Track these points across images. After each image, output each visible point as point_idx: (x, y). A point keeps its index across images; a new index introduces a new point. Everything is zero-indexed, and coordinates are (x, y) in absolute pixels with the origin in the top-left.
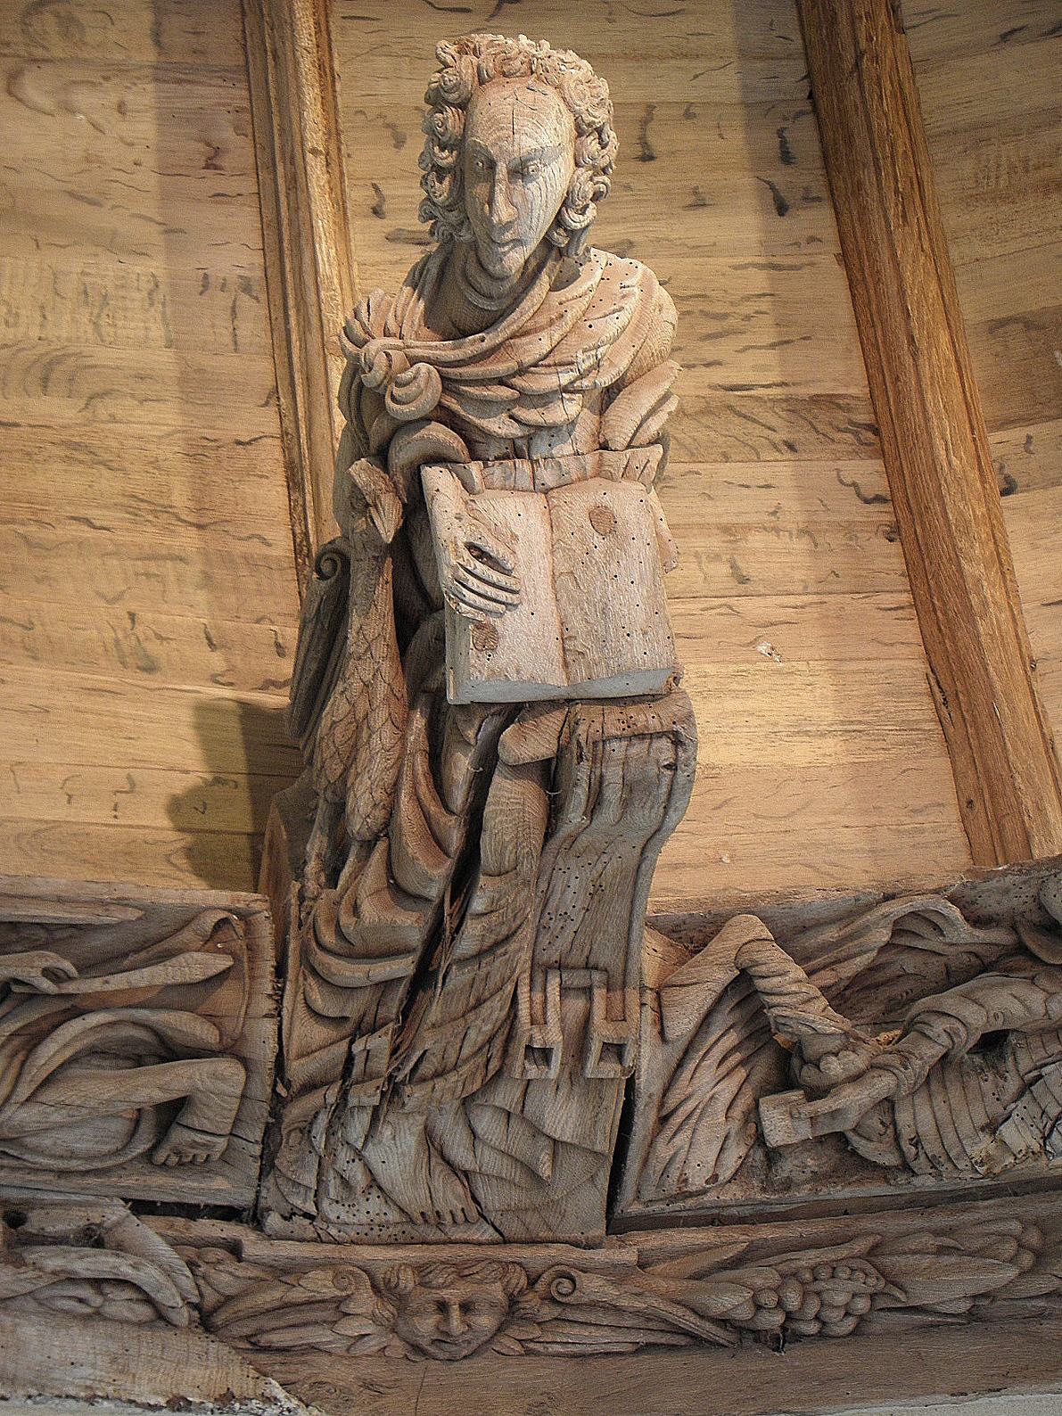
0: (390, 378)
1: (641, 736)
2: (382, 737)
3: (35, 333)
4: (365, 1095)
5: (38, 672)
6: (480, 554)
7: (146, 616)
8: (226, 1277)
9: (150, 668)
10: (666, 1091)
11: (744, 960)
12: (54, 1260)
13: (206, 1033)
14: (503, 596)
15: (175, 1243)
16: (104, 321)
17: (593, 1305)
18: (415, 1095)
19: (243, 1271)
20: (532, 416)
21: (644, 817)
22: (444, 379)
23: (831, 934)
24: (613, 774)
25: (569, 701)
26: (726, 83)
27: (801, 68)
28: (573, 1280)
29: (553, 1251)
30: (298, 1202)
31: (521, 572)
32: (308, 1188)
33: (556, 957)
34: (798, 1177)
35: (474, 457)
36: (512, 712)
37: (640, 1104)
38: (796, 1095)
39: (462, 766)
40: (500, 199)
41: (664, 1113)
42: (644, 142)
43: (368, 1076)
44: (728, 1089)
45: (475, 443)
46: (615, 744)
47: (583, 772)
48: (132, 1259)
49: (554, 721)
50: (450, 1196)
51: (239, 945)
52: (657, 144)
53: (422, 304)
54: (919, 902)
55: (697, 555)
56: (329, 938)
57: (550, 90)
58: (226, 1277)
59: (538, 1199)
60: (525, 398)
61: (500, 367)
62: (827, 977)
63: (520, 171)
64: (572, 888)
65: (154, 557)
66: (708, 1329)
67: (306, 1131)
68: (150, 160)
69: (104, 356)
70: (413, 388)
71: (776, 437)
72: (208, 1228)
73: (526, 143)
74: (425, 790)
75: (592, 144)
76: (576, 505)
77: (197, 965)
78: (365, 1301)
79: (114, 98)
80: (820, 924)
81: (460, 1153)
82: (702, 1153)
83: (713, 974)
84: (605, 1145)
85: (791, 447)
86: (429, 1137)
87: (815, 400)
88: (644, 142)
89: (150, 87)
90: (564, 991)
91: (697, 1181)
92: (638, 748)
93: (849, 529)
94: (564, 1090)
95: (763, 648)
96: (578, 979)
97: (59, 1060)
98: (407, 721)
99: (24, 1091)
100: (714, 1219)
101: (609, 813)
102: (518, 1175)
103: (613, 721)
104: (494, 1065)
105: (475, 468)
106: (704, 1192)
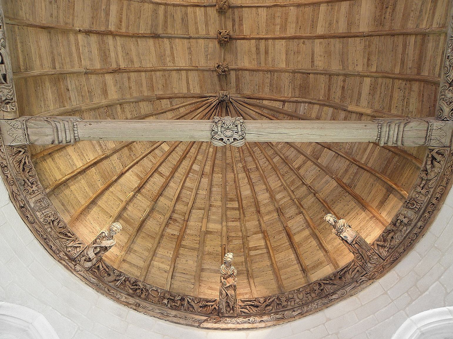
4: (365, 264)
8: (368, 277)
12: (359, 282)
13: (356, 266)
36: (352, 242)
50: (375, 265)
58: (368, 277)
64: (364, 247)
66: (393, 261)
76: (346, 231)
77: (353, 264)
78: (376, 273)
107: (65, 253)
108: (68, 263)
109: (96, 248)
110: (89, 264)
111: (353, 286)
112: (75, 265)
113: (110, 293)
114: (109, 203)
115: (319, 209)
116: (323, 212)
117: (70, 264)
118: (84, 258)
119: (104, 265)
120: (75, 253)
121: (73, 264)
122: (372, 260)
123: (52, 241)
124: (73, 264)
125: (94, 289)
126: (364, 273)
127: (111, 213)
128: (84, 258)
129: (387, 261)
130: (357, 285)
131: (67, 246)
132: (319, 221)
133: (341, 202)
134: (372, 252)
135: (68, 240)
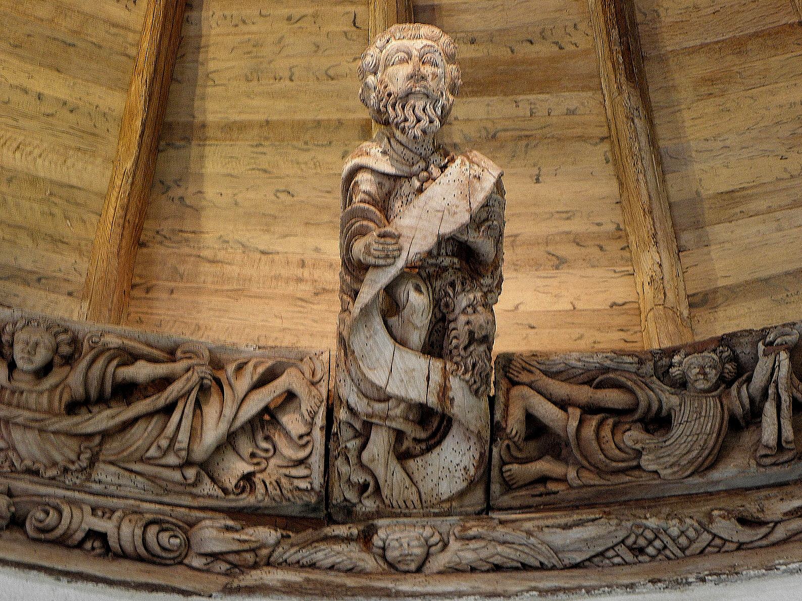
107: (232, 513)
108: (305, 555)
109: (390, 304)
110: (451, 463)
112: (366, 538)
113: (780, 533)
114: (281, 65)
117: (324, 554)
118: (379, 444)
119: (561, 389)
120: (289, 464)
121: (337, 539)
123: (71, 502)
124: (348, 539)
125: (632, 586)
127: (348, 110)
128: (379, 444)
131: (200, 452)
135: (168, 410)
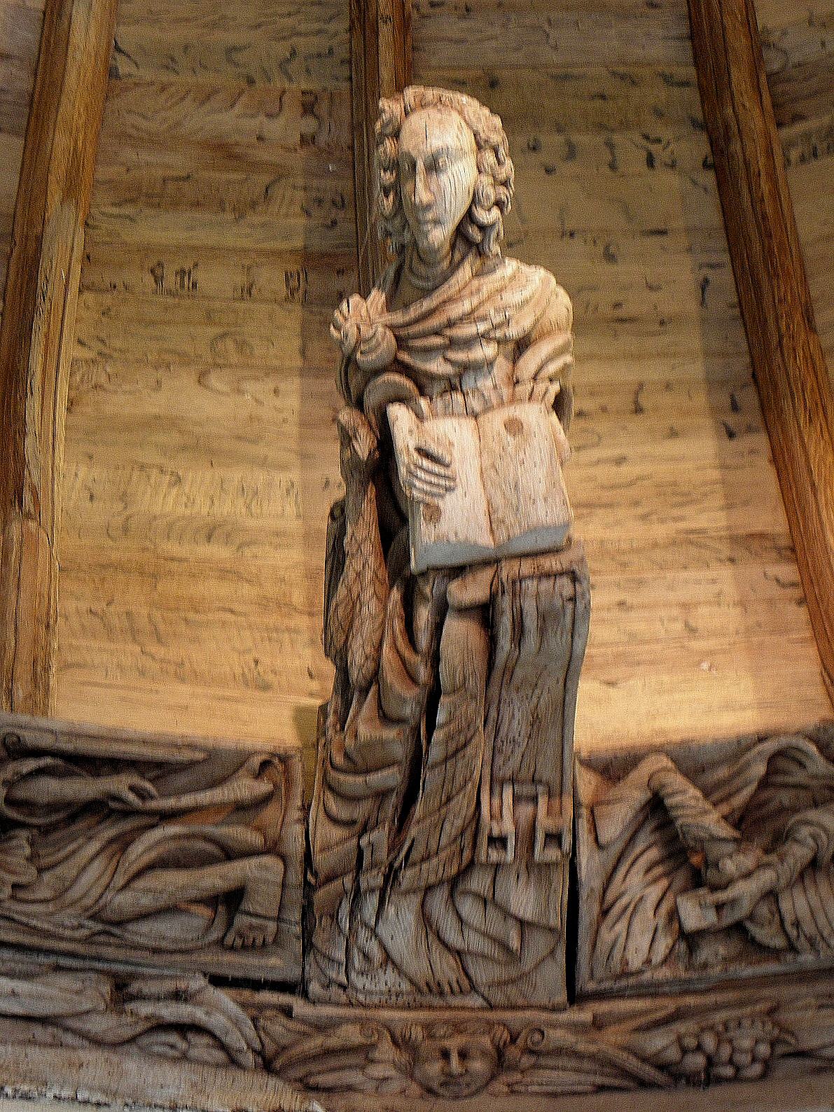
0: (359, 341)
1: (548, 575)
2: (370, 607)
3: (205, 511)
4: (373, 879)
5: (185, 689)
6: (423, 452)
7: (266, 660)
8: (278, 1028)
9: (266, 687)
10: (605, 891)
11: (655, 783)
12: (145, 1009)
13: (255, 839)
14: (442, 482)
15: (244, 1006)
16: (254, 503)
17: (559, 1052)
18: (408, 877)
19: (291, 1025)
20: (460, 356)
21: (557, 642)
22: (397, 338)
23: (722, 772)
24: (529, 606)
25: (497, 561)
26: (696, 370)
27: (747, 359)
28: (542, 1033)
29: (528, 1014)
30: (333, 975)
31: (456, 466)
32: (340, 964)
33: (509, 773)
34: (711, 960)
35: (422, 394)
36: (457, 571)
37: (584, 894)
38: (703, 891)
39: (424, 615)
40: (420, 185)
41: (605, 906)
42: (636, 402)
43: (374, 865)
44: (654, 893)
45: (423, 382)
46: (529, 582)
47: (505, 603)
48: (204, 1009)
49: (486, 575)
50: (446, 969)
51: (280, 778)
52: (644, 402)
53: (384, 295)
54: (784, 741)
55: (662, 620)
56: (339, 759)
57: (455, 115)
58: (278, 1028)
59: (514, 972)
60: (453, 344)
61: (434, 322)
62: (725, 809)
63: (434, 166)
64: (516, 720)
65: (277, 630)
66: (648, 1072)
67: (334, 917)
68: (294, 419)
69: (251, 523)
70: (374, 342)
71: (723, 557)
72: (267, 997)
73: (436, 143)
74: (401, 642)
75: (489, 158)
76: (495, 421)
77: (244, 788)
78: (386, 1050)
79: (271, 386)
80: (714, 765)
81: (452, 937)
82: (638, 940)
83: (632, 795)
84: (557, 919)
85: (732, 560)
86: (425, 919)
87: (752, 536)
88: (636, 402)
89: (297, 381)
90: (517, 799)
91: (635, 962)
92: (546, 585)
93: (771, 602)
94: (523, 878)
95: (705, 666)
96: (527, 790)
97: (146, 859)
98: (388, 596)
99: (120, 880)
100: (652, 991)
101: (531, 641)
102: (496, 952)
103: (527, 567)
104: (467, 854)
105: (423, 403)
106: (640, 972)
111: (52, 993)
115: (282, 50)
116: (292, 110)
122: (468, 908)
126: (277, 965)
129: (598, 1024)
130: (101, 1024)
132: (178, 162)
133: (567, 169)
134: (545, 822)
